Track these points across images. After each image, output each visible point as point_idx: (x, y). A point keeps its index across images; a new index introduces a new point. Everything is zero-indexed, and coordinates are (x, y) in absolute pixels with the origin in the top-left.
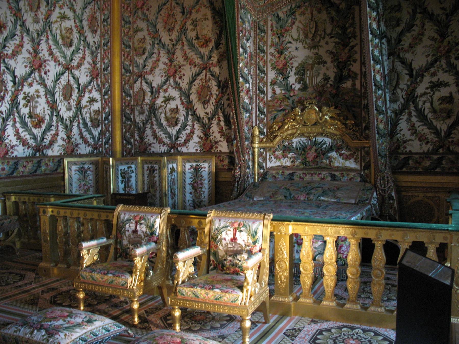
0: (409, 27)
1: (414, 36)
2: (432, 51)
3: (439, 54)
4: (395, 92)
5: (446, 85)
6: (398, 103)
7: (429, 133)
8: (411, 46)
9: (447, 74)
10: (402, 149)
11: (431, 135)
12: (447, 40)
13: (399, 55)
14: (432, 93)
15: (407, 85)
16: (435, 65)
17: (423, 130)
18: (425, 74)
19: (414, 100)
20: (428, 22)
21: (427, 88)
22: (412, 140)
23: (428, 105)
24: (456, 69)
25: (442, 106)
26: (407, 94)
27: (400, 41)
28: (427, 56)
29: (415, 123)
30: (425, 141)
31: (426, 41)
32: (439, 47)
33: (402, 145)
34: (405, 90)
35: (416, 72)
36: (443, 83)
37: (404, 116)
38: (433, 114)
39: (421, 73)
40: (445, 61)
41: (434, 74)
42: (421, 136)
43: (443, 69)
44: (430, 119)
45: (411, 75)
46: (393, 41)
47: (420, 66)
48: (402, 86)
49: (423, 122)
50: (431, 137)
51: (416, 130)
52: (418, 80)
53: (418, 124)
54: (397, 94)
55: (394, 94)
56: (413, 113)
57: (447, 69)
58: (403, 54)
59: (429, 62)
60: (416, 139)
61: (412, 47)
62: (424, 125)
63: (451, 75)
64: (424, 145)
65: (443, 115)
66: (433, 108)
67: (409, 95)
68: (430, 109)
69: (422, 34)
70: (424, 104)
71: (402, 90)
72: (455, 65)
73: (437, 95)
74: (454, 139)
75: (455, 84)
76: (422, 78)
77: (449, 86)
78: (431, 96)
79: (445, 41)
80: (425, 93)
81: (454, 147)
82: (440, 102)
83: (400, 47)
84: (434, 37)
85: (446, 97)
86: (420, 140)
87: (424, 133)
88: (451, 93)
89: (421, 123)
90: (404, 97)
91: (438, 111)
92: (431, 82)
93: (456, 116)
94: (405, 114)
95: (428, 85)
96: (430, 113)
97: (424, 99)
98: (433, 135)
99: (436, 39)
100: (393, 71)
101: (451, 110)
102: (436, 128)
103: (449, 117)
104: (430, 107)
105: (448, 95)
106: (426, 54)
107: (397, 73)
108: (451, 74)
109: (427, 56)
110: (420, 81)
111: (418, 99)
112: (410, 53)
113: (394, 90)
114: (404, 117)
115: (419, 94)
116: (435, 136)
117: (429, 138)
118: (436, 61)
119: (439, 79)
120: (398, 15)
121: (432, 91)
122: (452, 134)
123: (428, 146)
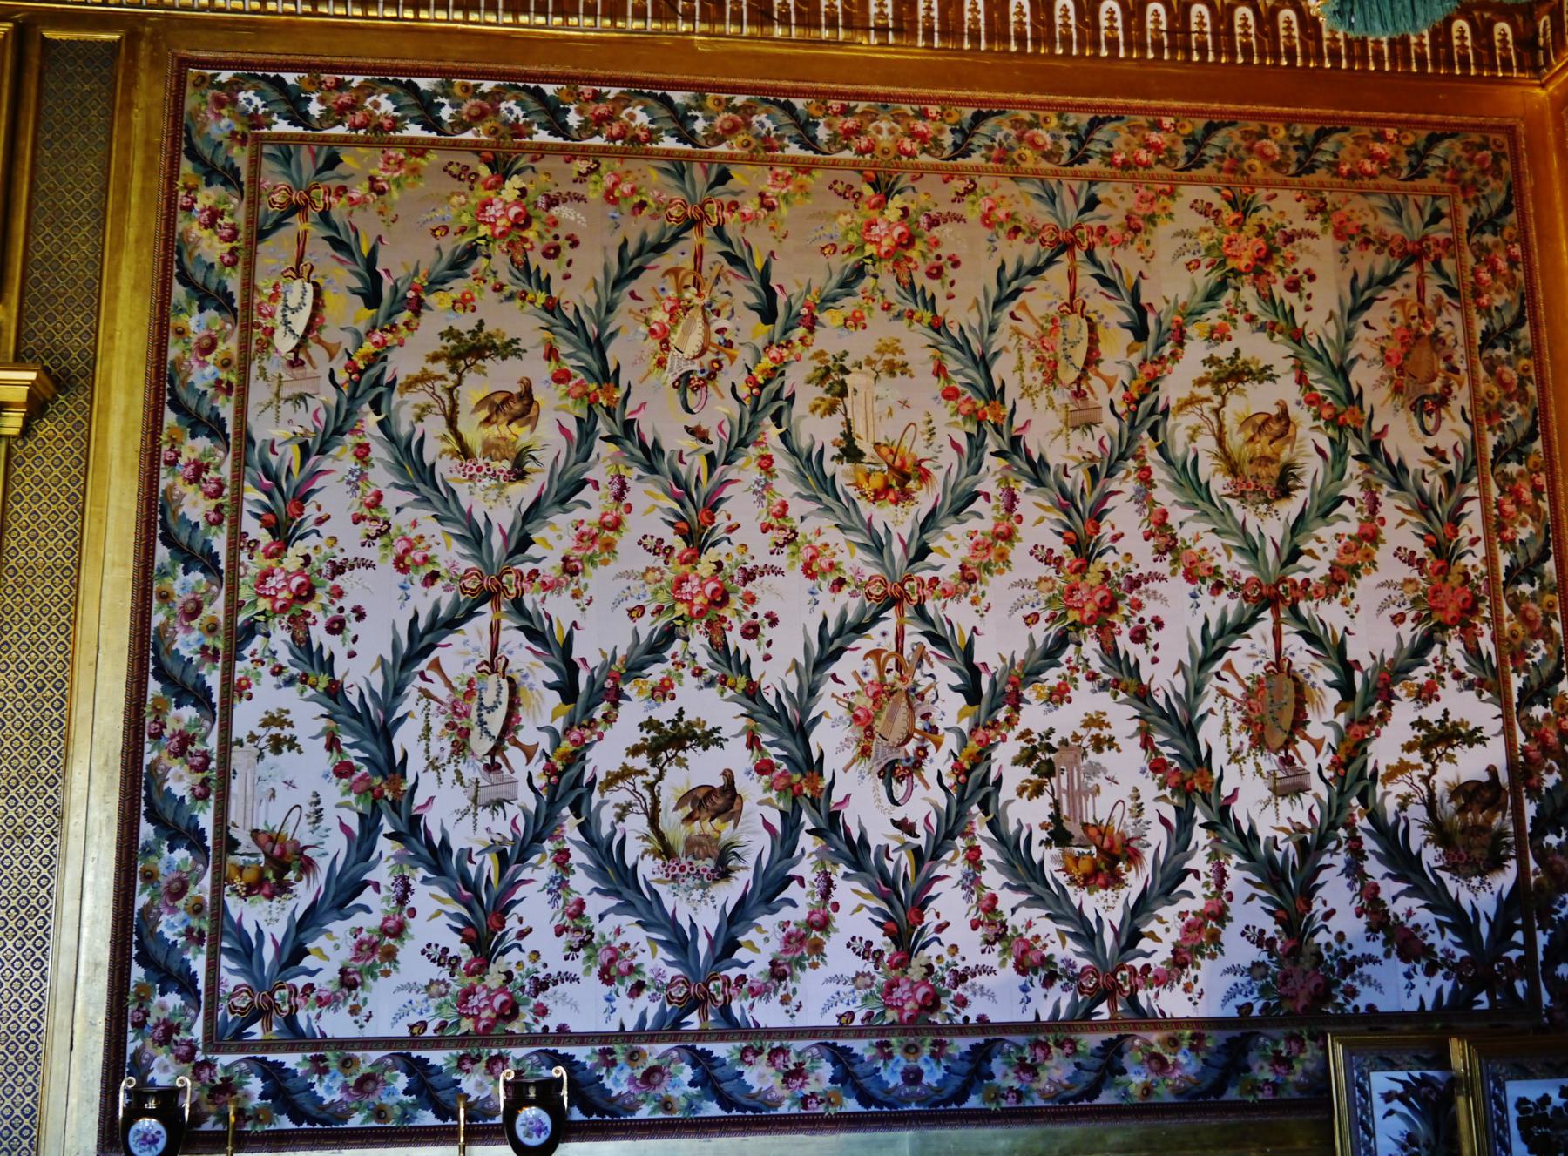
0: (568, 490)
1: (585, 528)
2: (655, 593)
3: (681, 609)
4: (498, 759)
5: (710, 739)
6: (512, 810)
7: (645, 945)
8: (570, 568)
9: (713, 692)
10: (529, 1019)
11: (654, 953)
12: (711, 555)
13: (518, 604)
14: (656, 771)
15: (552, 731)
16: (668, 654)
17: (618, 931)
18: (627, 689)
19: (580, 798)
20: (639, 478)
21: (635, 751)
22: (573, 979)
23: (637, 823)
24: (749, 675)
25: (696, 826)
26: (550, 770)
27: (525, 542)
28: (637, 612)
29: (587, 899)
30: (630, 982)
31: (630, 554)
32: (681, 581)
33: (527, 1003)
34: (544, 752)
35: (591, 681)
36: (699, 732)
37: (535, 866)
38: (659, 861)
39: (609, 684)
40: (706, 641)
41: (663, 691)
42: (611, 961)
43: (698, 673)
44: (647, 883)
45: (567, 690)
46: (497, 541)
47: (604, 655)
48: (527, 735)
49: (618, 894)
50: (655, 962)
51: (590, 932)
52: (598, 714)
53: (597, 904)
54: (504, 768)
55: (492, 768)
56: (578, 857)
57: (714, 673)
58: (538, 598)
59: (643, 638)
60: (588, 970)
61: (574, 572)
62: (626, 907)
63: (731, 699)
64: (623, 1001)
65: (700, 864)
66: (660, 836)
67: (560, 774)
68: (646, 838)
69: (616, 525)
70: (621, 818)
71: (529, 753)
72: (743, 659)
73: (676, 782)
74: (749, 972)
75: (744, 739)
76: (616, 705)
77: (719, 742)
78: (650, 787)
79: (703, 558)
80: (626, 773)
81: (746, 1004)
82: (688, 809)
83: (526, 568)
84: (661, 541)
85: (711, 791)
86: (606, 977)
87: (626, 946)
88: (729, 776)
89: (613, 902)
90: (539, 782)
91: (680, 849)
92: (650, 724)
93: (751, 872)
94: (542, 860)
95: (637, 737)
96: (649, 858)
97: (620, 795)
98: (661, 952)
99: (672, 548)
100: (494, 671)
101: (731, 845)
102: (673, 921)
103: (723, 873)
104: (648, 830)
105: (719, 782)
106: (633, 603)
107: (511, 680)
108: (729, 693)
109: (637, 612)
110: (605, 716)
111: (596, 797)
112: (567, 594)
113: (492, 753)
114: (537, 875)
115: (601, 777)
116: (671, 958)
117: (645, 969)
118: (669, 635)
119: (681, 712)
120: (520, 434)
121: (654, 763)
122: (739, 945)
123: (643, 1000)
